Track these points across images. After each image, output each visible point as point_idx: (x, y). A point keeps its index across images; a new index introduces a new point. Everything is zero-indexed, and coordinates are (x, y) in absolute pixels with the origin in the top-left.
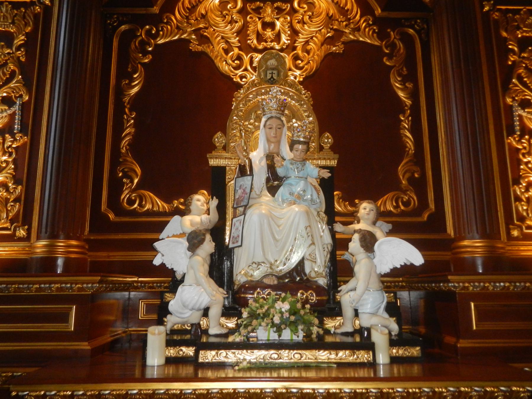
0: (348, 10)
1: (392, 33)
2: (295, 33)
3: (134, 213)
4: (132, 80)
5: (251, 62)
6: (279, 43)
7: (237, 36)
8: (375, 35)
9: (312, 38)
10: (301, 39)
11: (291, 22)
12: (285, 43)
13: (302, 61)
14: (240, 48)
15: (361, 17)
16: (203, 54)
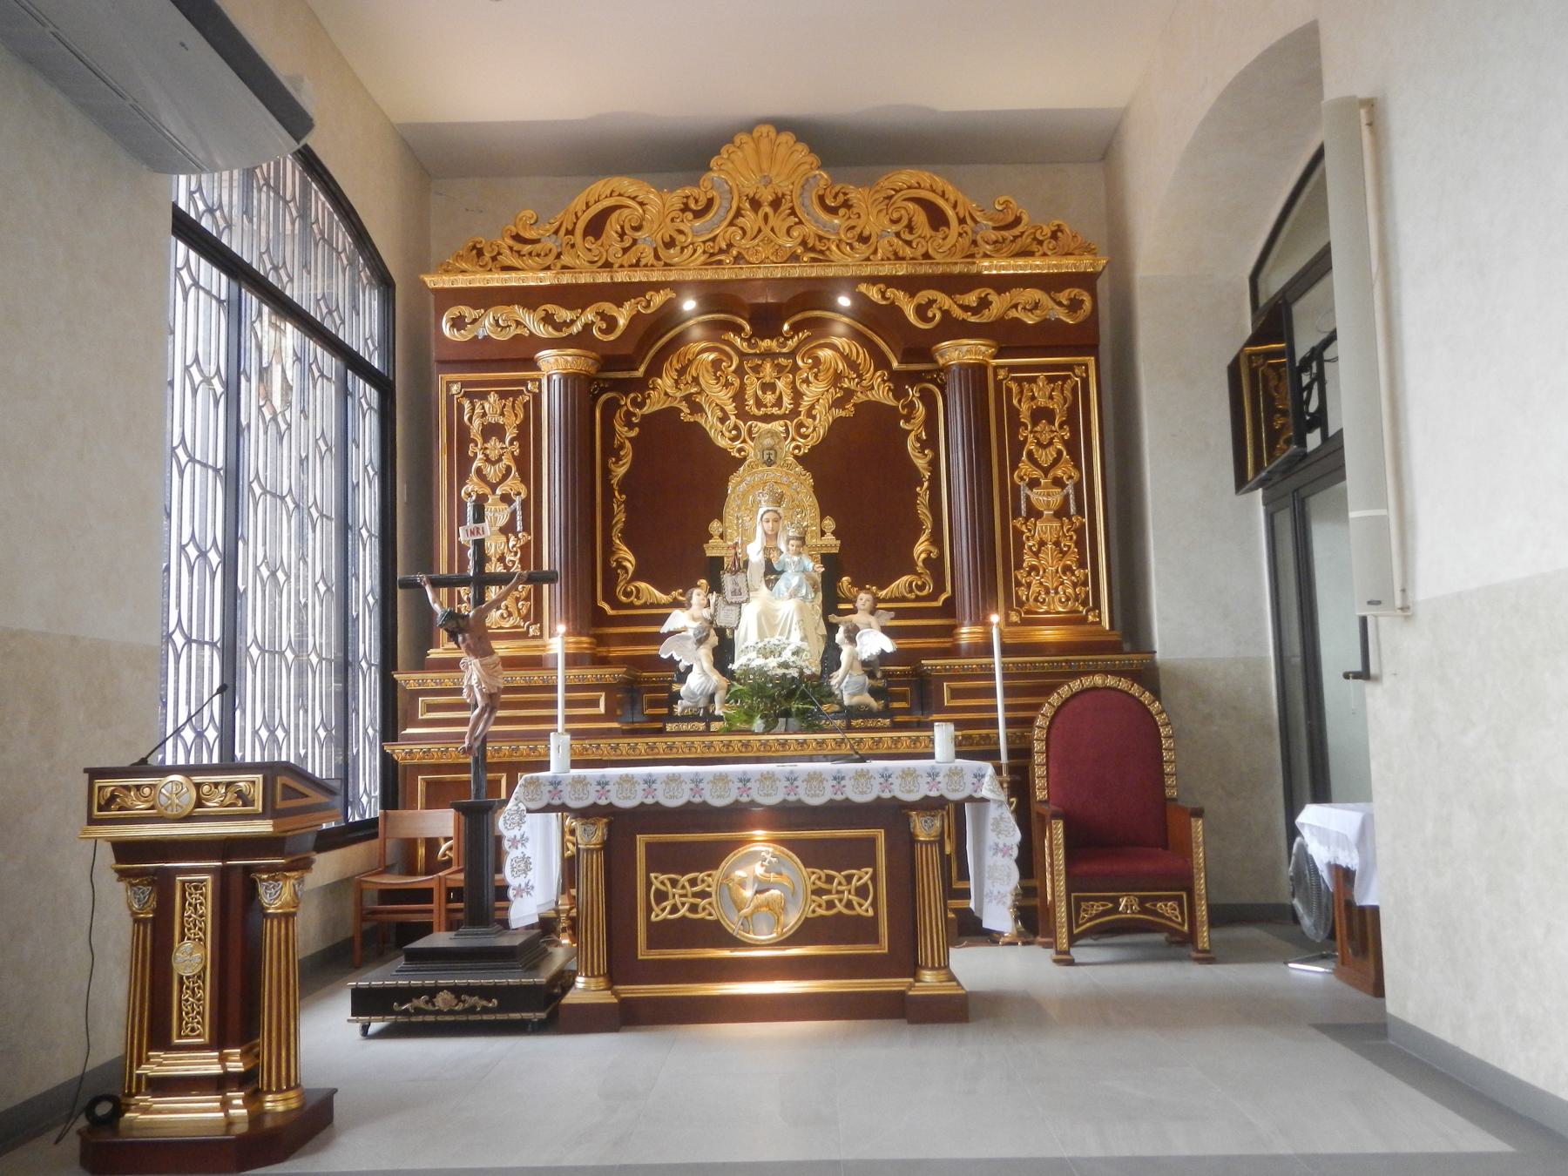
0: (860, 364)
1: (910, 390)
3: (631, 606)
4: (619, 459)
7: (733, 401)
8: (891, 394)
9: (818, 400)
10: (806, 403)
11: (794, 382)
12: (787, 408)
13: (807, 428)
15: (875, 371)
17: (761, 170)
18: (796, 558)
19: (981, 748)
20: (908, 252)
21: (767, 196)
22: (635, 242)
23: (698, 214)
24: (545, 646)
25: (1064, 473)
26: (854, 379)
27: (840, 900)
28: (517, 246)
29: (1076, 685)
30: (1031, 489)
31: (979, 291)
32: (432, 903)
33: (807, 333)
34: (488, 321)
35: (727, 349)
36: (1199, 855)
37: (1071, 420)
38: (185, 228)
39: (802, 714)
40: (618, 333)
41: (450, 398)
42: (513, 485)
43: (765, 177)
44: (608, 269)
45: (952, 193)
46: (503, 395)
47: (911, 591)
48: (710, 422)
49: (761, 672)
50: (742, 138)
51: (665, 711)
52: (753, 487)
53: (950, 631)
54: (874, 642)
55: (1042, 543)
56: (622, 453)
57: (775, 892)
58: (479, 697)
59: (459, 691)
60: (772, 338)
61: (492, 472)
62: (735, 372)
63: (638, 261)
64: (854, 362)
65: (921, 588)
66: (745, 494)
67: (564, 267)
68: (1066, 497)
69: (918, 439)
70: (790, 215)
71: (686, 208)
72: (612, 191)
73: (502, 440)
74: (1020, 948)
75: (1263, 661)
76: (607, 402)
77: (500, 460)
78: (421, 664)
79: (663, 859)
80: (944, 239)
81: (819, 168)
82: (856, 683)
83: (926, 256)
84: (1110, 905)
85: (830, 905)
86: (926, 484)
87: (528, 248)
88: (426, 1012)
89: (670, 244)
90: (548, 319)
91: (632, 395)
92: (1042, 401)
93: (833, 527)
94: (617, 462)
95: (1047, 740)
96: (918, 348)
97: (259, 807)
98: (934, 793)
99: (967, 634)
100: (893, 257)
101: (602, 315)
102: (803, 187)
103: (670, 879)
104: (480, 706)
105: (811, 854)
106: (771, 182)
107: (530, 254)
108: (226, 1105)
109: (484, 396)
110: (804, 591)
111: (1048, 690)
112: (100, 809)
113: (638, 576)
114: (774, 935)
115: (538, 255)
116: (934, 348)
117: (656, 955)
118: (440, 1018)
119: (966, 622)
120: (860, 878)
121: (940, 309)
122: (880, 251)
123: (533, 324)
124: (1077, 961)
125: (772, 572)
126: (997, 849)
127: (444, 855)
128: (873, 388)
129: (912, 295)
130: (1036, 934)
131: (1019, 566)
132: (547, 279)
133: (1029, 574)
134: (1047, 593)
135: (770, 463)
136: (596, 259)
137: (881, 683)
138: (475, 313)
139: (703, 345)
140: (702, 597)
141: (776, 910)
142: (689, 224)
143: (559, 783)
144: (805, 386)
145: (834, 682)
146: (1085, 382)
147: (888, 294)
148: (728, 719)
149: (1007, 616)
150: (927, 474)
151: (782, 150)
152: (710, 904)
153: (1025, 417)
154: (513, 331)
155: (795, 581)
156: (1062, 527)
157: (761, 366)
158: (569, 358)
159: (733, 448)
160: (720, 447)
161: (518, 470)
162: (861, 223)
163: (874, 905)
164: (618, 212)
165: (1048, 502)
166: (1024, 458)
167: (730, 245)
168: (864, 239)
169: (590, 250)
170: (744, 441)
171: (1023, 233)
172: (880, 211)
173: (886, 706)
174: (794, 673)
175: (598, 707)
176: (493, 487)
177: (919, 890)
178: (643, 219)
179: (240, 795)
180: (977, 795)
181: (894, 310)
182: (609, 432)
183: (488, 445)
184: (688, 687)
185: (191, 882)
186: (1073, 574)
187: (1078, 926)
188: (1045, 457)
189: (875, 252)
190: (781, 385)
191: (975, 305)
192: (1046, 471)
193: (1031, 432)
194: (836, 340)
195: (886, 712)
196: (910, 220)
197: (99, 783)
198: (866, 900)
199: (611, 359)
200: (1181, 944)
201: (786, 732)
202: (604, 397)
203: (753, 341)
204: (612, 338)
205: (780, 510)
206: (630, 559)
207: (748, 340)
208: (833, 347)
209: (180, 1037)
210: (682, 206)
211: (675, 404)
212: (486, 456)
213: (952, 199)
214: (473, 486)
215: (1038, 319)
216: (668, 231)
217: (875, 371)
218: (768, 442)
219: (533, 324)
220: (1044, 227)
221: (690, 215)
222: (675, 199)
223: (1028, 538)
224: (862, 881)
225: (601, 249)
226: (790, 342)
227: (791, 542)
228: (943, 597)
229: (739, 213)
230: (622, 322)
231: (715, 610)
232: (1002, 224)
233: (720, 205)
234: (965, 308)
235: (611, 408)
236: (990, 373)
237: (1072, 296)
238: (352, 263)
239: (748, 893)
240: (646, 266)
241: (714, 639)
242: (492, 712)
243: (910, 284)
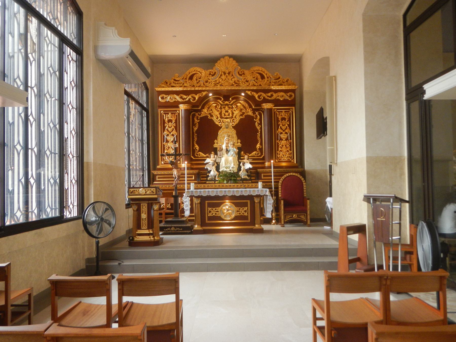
2: (233, 114)
3: (198, 157)
5: (223, 121)
6: (229, 116)
9: (237, 115)
10: (234, 115)
11: (232, 111)
14: (220, 118)
15: (249, 108)
16: (212, 119)
17: (226, 66)
18: (232, 148)
19: (269, 187)
20: (256, 84)
22: (199, 81)
23: (213, 75)
24: (181, 166)
25: (288, 131)
26: (245, 110)
27: (242, 213)
28: (175, 82)
29: (287, 175)
30: (281, 134)
31: (271, 93)
32: (162, 215)
33: (235, 100)
34: (169, 98)
35: (218, 103)
36: (309, 207)
37: (289, 120)
38: (126, 93)
39: (234, 180)
40: (196, 100)
41: (161, 114)
42: (174, 132)
43: (227, 67)
44: (194, 87)
45: (266, 72)
46: (172, 113)
47: (256, 155)
48: (214, 119)
49: (226, 171)
50: (222, 59)
51: (206, 179)
52: (223, 133)
53: (264, 163)
54: (248, 166)
55: (283, 146)
56: (196, 125)
58: (176, 176)
59: (173, 175)
60: (228, 101)
61: (169, 129)
62: (220, 108)
63: (200, 85)
64: (245, 106)
65: (258, 154)
66: (221, 135)
67: (185, 86)
68: (288, 136)
69: (258, 123)
70: (232, 76)
71: (210, 74)
72: (195, 70)
73: (172, 123)
74: (275, 225)
75: (327, 170)
76: (193, 114)
77: (171, 127)
78: (155, 169)
79: (210, 205)
80: (264, 81)
81: (238, 66)
82: (244, 174)
83: (260, 85)
84: (292, 216)
85: (240, 213)
86: (259, 132)
87: (177, 82)
88: (170, 231)
89: (207, 82)
90: (181, 98)
91: (198, 113)
92: (283, 116)
93: (240, 141)
94: (195, 127)
95: (282, 185)
96: (258, 104)
97: (155, 193)
98: (258, 194)
99: (267, 164)
100: (253, 85)
101: (193, 97)
102: (235, 70)
103: (211, 209)
104: (177, 178)
105: (236, 205)
106: (228, 69)
107: (177, 83)
108: (150, 238)
109: (168, 114)
110: (234, 155)
112: (131, 193)
113: (199, 151)
114: (230, 219)
115: (179, 84)
116: (261, 105)
118: (172, 232)
119: (267, 161)
120: (245, 209)
121: (263, 96)
122: (251, 84)
123: (178, 98)
124: (285, 226)
125: (227, 151)
126: (269, 204)
127: (162, 207)
128: (249, 112)
129: (257, 93)
130: (278, 222)
131: (278, 150)
132: (181, 89)
133: (280, 152)
134: (283, 156)
135: (227, 128)
136: (191, 85)
137: (249, 174)
138: (166, 96)
139: (213, 102)
140: (213, 156)
141: (230, 214)
142: (211, 77)
143: (193, 192)
144: (234, 111)
147: (252, 93)
148: (219, 181)
149: (275, 160)
150: (260, 131)
151: (230, 62)
152: (219, 213)
153: (280, 120)
154: (174, 100)
155: (232, 153)
156: (287, 142)
157: (225, 107)
158: (186, 106)
159: (219, 125)
160: (216, 124)
161: (175, 129)
162: (247, 78)
163: (248, 213)
164: (196, 75)
165: (284, 137)
166: (279, 128)
167: (219, 82)
168: (247, 81)
169: (190, 83)
170: (222, 123)
171: (280, 80)
172: (251, 75)
173: (250, 178)
175: (193, 178)
177: (255, 211)
178: (201, 76)
179: (152, 191)
180: (266, 194)
181: (253, 97)
182: (193, 121)
183: (169, 124)
184: (211, 174)
185: (143, 205)
186: (289, 152)
187: (286, 220)
188: (284, 128)
189: (250, 84)
190: (230, 111)
191: (270, 96)
192: (284, 131)
193: (281, 122)
194: (241, 102)
195: (250, 180)
196: (257, 77)
197: (130, 189)
198: (246, 213)
199: (194, 105)
200: (305, 223)
201: (231, 183)
202: (192, 113)
203: (224, 102)
204: (194, 102)
205: (229, 138)
206: (197, 147)
207: (223, 101)
208: (240, 103)
209: (142, 228)
210: (209, 74)
211: (207, 115)
212: (169, 126)
213: (266, 73)
214: (166, 132)
215: (283, 99)
216: (206, 79)
217: (249, 108)
218: (227, 123)
219: (178, 98)
220: (285, 79)
221: (211, 76)
222: (208, 72)
223: (280, 145)
224: (245, 209)
225: (192, 83)
226: (231, 102)
227: (232, 145)
228: (263, 156)
229: (221, 75)
230: (197, 98)
231: (216, 159)
232: (276, 78)
233: (217, 74)
234: (268, 96)
236: (273, 110)
237: (290, 94)
238: (142, 86)
239: (225, 211)
240: (202, 86)
241: (216, 165)
242: (179, 179)
243: (257, 91)
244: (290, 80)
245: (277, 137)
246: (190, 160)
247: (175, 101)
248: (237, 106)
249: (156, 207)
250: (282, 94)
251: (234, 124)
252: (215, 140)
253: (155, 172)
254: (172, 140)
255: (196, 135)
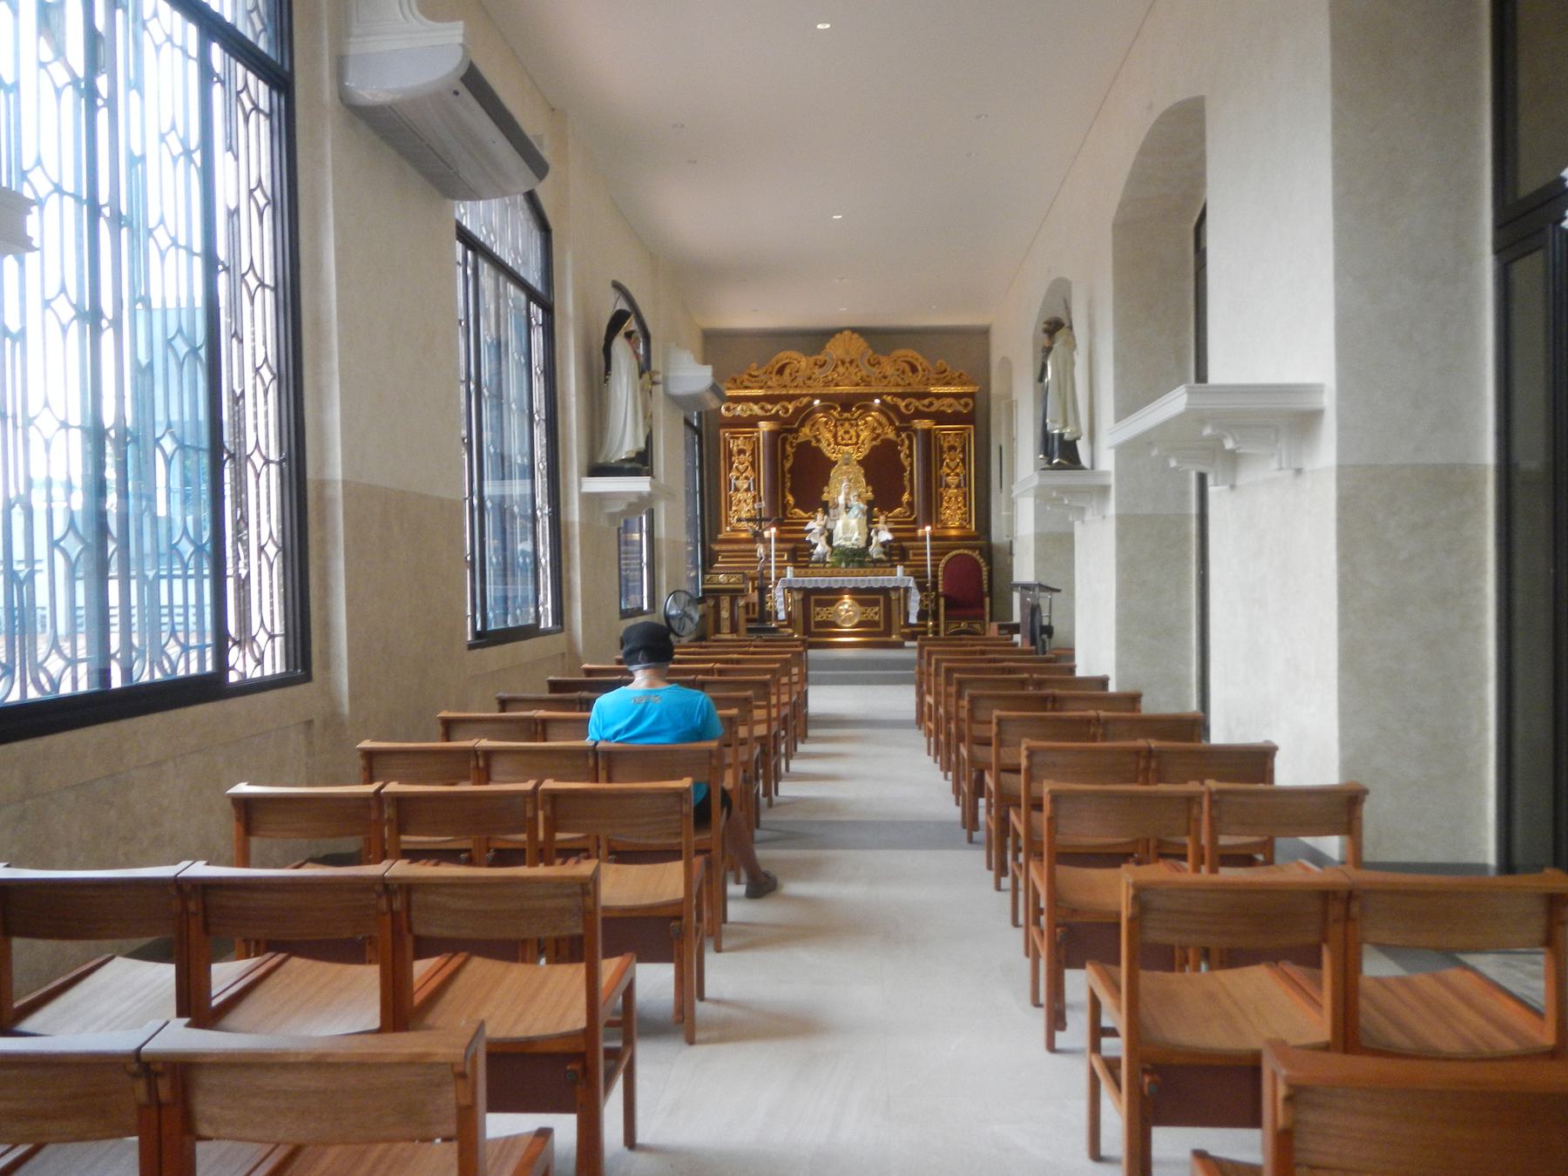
3: (792, 518)
10: (862, 438)
21: (848, 360)
23: (821, 366)
28: (750, 378)
29: (954, 553)
34: (739, 408)
37: (963, 451)
39: (860, 562)
41: (725, 439)
45: (920, 357)
48: (823, 445)
49: (843, 546)
52: (841, 474)
53: (915, 530)
54: (885, 536)
55: (950, 498)
57: (851, 613)
60: (848, 412)
61: (740, 467)
67: (769, 387)
69: (905, 454)
71: (816, 364)
76: (782, 439)
79: (819, 603)
87: (754, 379)
90: (762, 408)
92: (952, 443)
99: (920, 532)
101: (783, 407)
105: (862, 603)
111: (947, 553)
113: (796, 506)
117: (816, 630)
123: (756, 409)
125: (848, 508)
131: (941, 506)
132: (760, 392)
135: (847, 464)
137: (887, 550)
141: (850, 619)
142: (817, 371)
145: (870, 550)
146: (969, 435)
153: (945, 449)
154: (748, 413)
155: (856, 512)
159: (833, 457)
168: (885, 377)
174: (856, 547)
176: (742, 473)
181: (895, 408)
182: (784, 450)
188: (952, 465)
190: (853, 432)
192: (953, 470)
202: (781, 436)
204: (787, 415)
214: (733, 474)
216: (809, 372)
218: (847, 456)
219: (756, 409)
221: (817, 367)
222: (812, 359)
229: (836, 366)
234: (924, 406)
235: (784, 440)
236: (932, 432)
239: (843, 613)
241: (826, 534)
243: (903, 396)
244: (965, 374)
245: (939, 480)
246: (779, 524)
247: (751, 416)
248: (866, 423)
249: (742, 602)
250: (950, 400)
251: (860, 456)
252: (823, 487)
253: (717, 547)
254: (746, 486)
255: (788, 476)
